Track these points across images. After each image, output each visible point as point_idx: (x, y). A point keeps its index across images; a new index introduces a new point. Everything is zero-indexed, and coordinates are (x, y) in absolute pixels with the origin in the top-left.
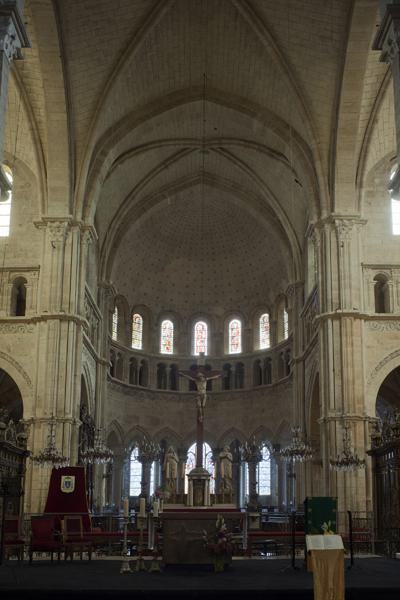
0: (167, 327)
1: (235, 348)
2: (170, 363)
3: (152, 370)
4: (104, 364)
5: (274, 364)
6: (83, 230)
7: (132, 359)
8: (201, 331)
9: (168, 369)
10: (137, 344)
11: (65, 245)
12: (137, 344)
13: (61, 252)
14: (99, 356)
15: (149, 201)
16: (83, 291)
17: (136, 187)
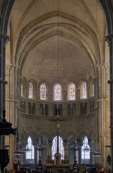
0: (43, 88)
1: (72, 97)
2: (45, 103)
3: (37, 107)
4: (20, 110)
5: (88, 105)
6: (15, 68)
7: (29, 103)
8: (58, 89)
9: (44, 106)
10: (31, 96)
11: (9, 74)
12: (31, 96)
13: (8, 77)
14: (18, 107)
15: (37, 43)
16: (16, 89)
17: (31, 39)
